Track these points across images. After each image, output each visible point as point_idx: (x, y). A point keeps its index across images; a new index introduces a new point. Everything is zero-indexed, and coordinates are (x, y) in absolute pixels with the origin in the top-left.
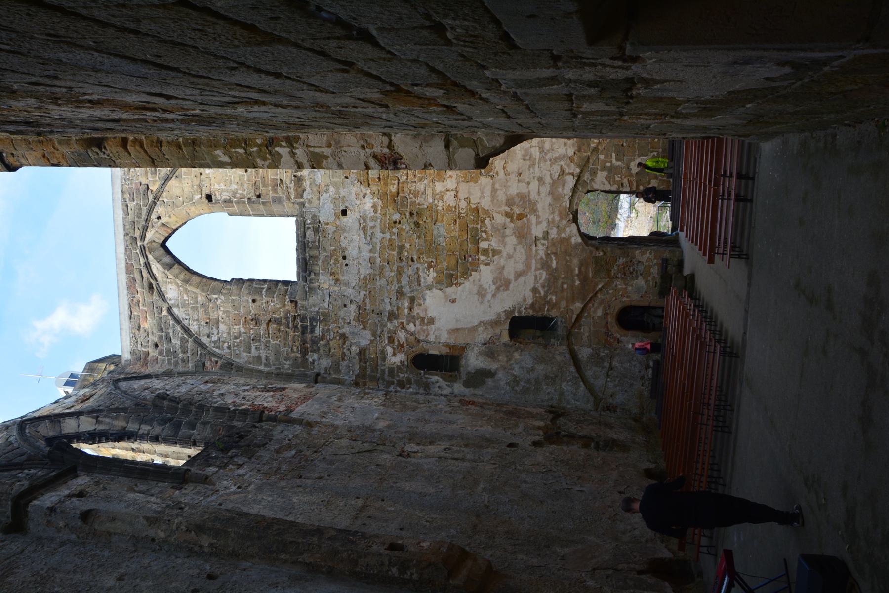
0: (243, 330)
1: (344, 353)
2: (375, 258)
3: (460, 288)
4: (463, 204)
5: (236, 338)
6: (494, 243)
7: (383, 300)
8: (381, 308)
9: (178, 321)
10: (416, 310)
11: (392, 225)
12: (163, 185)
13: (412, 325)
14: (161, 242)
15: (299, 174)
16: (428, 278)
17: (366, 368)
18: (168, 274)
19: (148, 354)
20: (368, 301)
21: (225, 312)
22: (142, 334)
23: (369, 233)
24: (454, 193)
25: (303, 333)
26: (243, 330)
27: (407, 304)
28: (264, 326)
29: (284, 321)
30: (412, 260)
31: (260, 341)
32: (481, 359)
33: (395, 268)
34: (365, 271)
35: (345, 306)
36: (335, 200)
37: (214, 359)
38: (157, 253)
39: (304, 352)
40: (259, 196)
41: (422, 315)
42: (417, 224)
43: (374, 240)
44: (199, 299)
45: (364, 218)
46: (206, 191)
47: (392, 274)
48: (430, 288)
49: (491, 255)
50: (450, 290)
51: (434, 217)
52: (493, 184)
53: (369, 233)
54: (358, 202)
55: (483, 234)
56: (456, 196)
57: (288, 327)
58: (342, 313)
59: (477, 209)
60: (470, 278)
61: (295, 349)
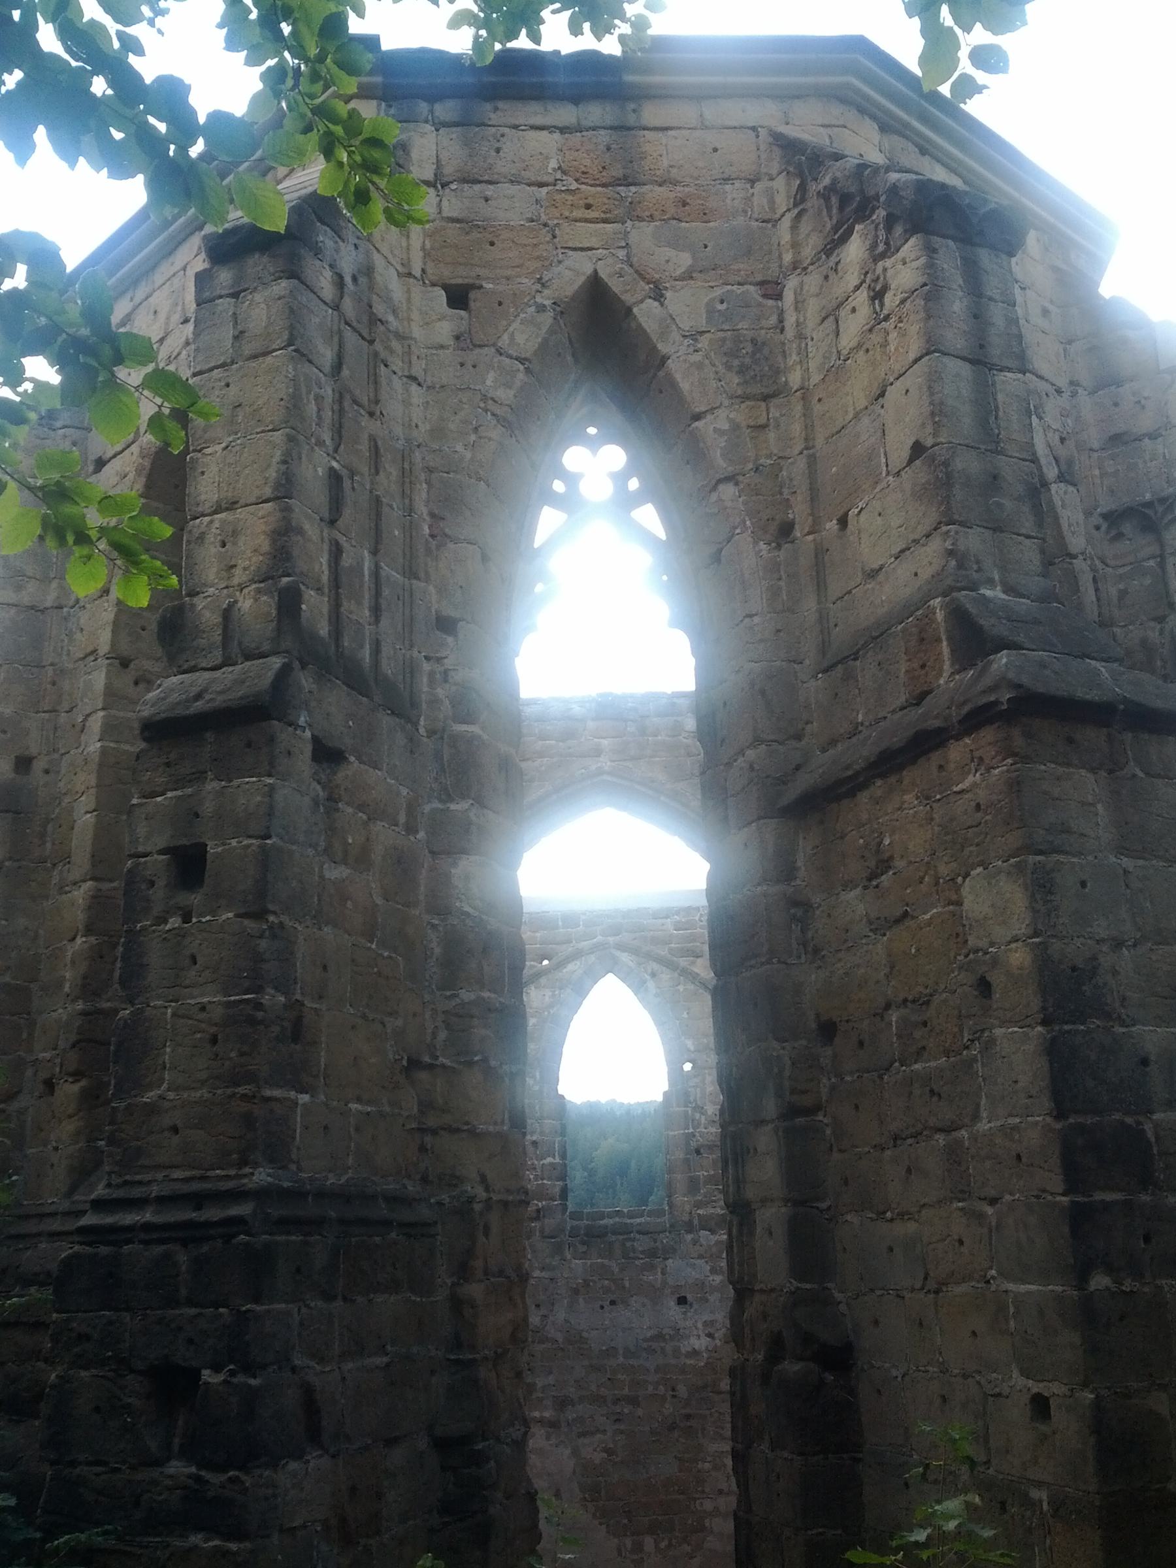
4: (708, 1505)
23: (655, 1345)
27: (547, 1414)
36: (701, 1285)
42: (672, 1427)
45: (678, 1334)
47: (593, 1388)
48: (575, 1453)
49: (635, 1557)
53: (655, 1345)
54: (700, 1325)
56: (721, 1492)
60: (596, 1522)
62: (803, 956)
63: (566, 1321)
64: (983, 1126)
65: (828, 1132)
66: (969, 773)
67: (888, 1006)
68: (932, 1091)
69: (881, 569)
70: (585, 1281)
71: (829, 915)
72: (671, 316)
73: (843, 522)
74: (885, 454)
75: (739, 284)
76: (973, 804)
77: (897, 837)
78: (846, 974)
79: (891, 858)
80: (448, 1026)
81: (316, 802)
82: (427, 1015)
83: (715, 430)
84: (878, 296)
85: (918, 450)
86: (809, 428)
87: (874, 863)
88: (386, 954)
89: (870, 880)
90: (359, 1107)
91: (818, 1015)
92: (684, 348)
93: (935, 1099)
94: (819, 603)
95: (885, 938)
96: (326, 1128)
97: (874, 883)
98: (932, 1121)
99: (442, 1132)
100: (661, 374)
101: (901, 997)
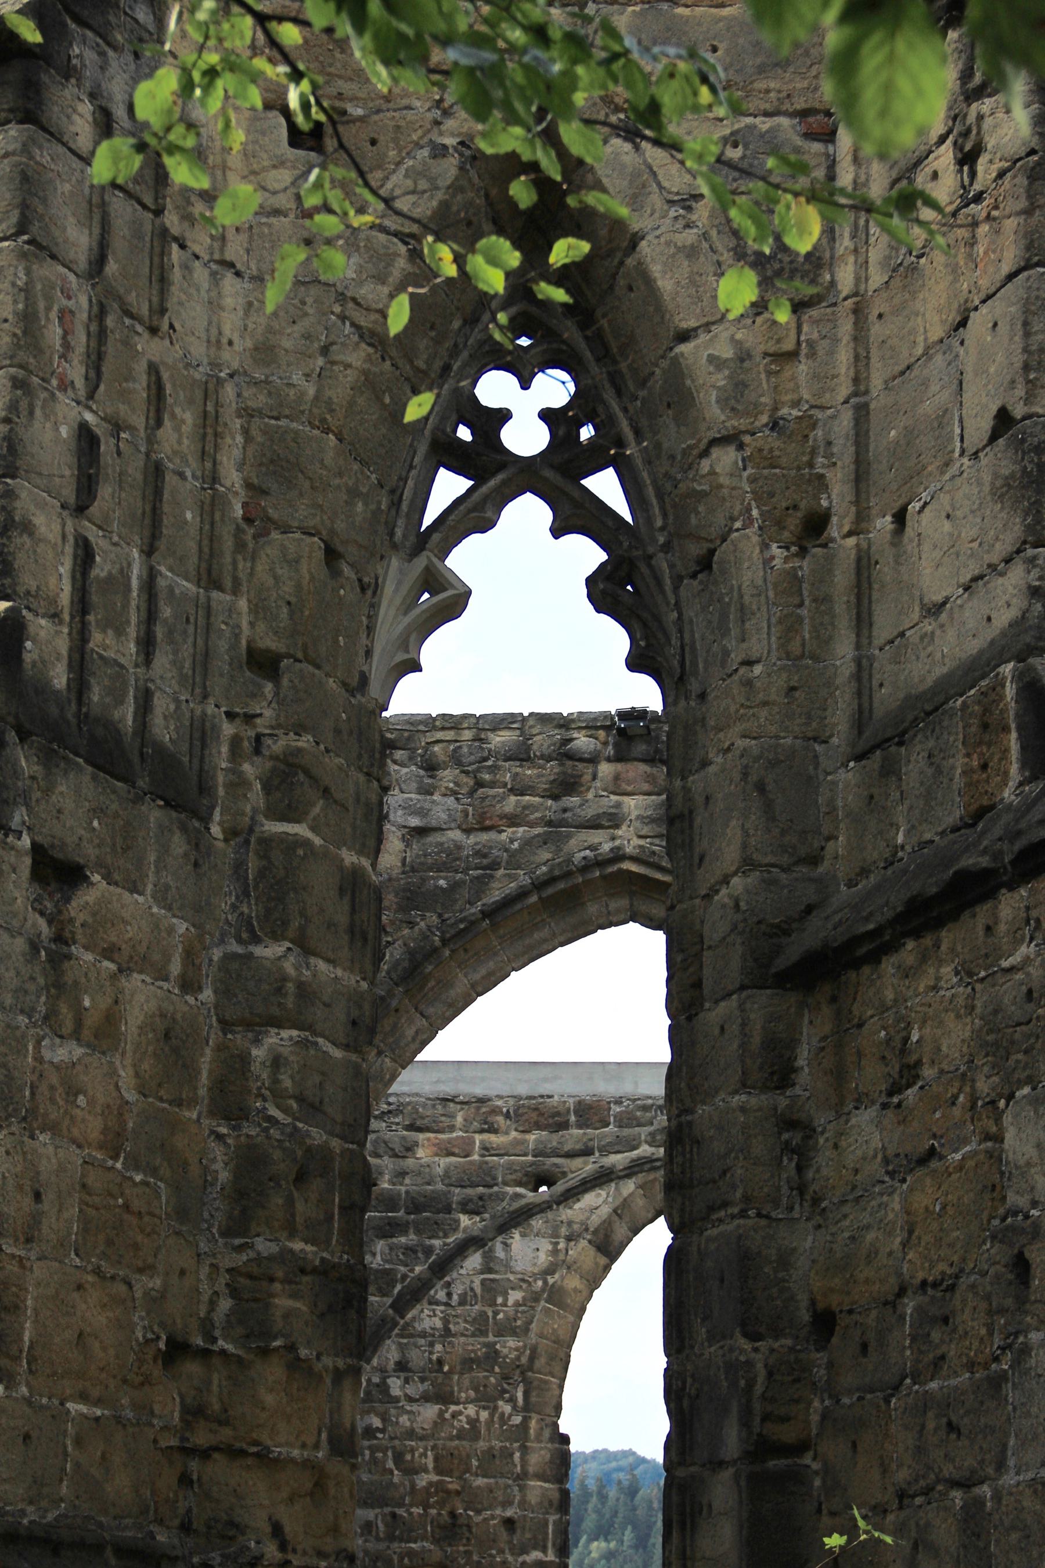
0: (422, 1481)
9: (442, 1267)
18: (583, 1243)
21: (474, 1422)
26: (422, 1481)
31: (391, 1538)
44: (512, 1342)
62: (797, 1207)
64: (1009, 1479)
65: (817, 1482)
66: (1023, 940)
67: (902, 1292)
68: (950, 1425)
69: (944, 604)
71: (836, 1146)
72: (650, 168)
73: (900, 518)
74: (961, 421)
75: (767, 114)
76: (1024, 988)
77: (927, 1030)
78: (853, 1238)
79: (919, 1063)
80: (234, 1292)
81: (34, 947)
82: (204, 1271)
83: (712, 359)
84: (967, 159)
85: (1004, 420)
86: (861, 361)
87: (897, 1068)
88: (138, 1178)
89: (890, 1094)
90: (83, 1408)
91: (813, 1302)
92: (668, 221)
93: (953, 1436)
94: (858, 646)
95: (905, 1186)
96: (27, 1437)
97: (895, 1100)
98: (948, 1470)
99: (216, 1455)
100: (630, 262)
101: (920, 1275)
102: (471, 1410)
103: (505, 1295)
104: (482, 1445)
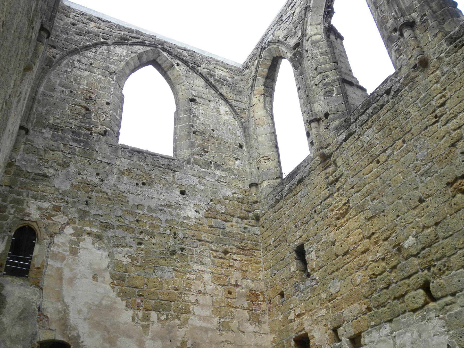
0: (82, 87)
1: (48, 161)
2: (143, 210)
3: (108, 287)
4: (192, 299)
5: (75, 80)
6: (155, 327)
7: (100, 209)
8: (93, 206)
10: (89, 239)
11: (173, 231)
12: (202, 75)
13: (72, 231)
14: (158, 60)
15: (212, 165)
16: (121, 255)
17: (26, 178)
18: (135, 54)
19: (68, 16)
20: (101, 195)
21: (100, 79)
22: (85, 20)
23: (166, 209)
24: (202, 289)
25: (73, 132)
27: (95, 230)
28: (84, 104)
29: (87, 120)
30: (140, 244)
32: (20, 304)
33: (132, 225)
34: (132, 199)
35: (98, 174)
36: (193, 187)
37: (58, 57)
38: (150, 54)
39: (53, 128)
40: (194, 133)
41: (82, 244)
42: (173, 253)
43: (160, 212)
44: (113, 66)
45: (179, 207)
46: (198, 100)
48: (111, 255)
49: (143, 323)
50: (107, 276)
51: (180, 270)
52: (212, 330)
53: (166, 209)
54: (192, 205)
55: (164, 317)
56: (200, 292)
57: (80, 122)
58: (91, 169)
59: (188, 312)
60: (120, 299)
61: (59, 121)
63: (115, 185)
70: (129, 169)
102: (100, 76)
103: (113, 57)
104: (102, 85)
